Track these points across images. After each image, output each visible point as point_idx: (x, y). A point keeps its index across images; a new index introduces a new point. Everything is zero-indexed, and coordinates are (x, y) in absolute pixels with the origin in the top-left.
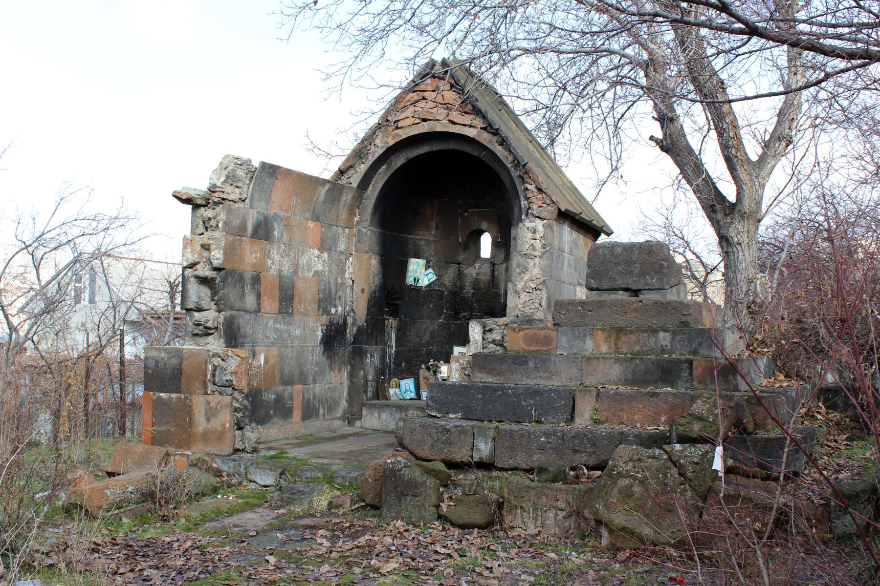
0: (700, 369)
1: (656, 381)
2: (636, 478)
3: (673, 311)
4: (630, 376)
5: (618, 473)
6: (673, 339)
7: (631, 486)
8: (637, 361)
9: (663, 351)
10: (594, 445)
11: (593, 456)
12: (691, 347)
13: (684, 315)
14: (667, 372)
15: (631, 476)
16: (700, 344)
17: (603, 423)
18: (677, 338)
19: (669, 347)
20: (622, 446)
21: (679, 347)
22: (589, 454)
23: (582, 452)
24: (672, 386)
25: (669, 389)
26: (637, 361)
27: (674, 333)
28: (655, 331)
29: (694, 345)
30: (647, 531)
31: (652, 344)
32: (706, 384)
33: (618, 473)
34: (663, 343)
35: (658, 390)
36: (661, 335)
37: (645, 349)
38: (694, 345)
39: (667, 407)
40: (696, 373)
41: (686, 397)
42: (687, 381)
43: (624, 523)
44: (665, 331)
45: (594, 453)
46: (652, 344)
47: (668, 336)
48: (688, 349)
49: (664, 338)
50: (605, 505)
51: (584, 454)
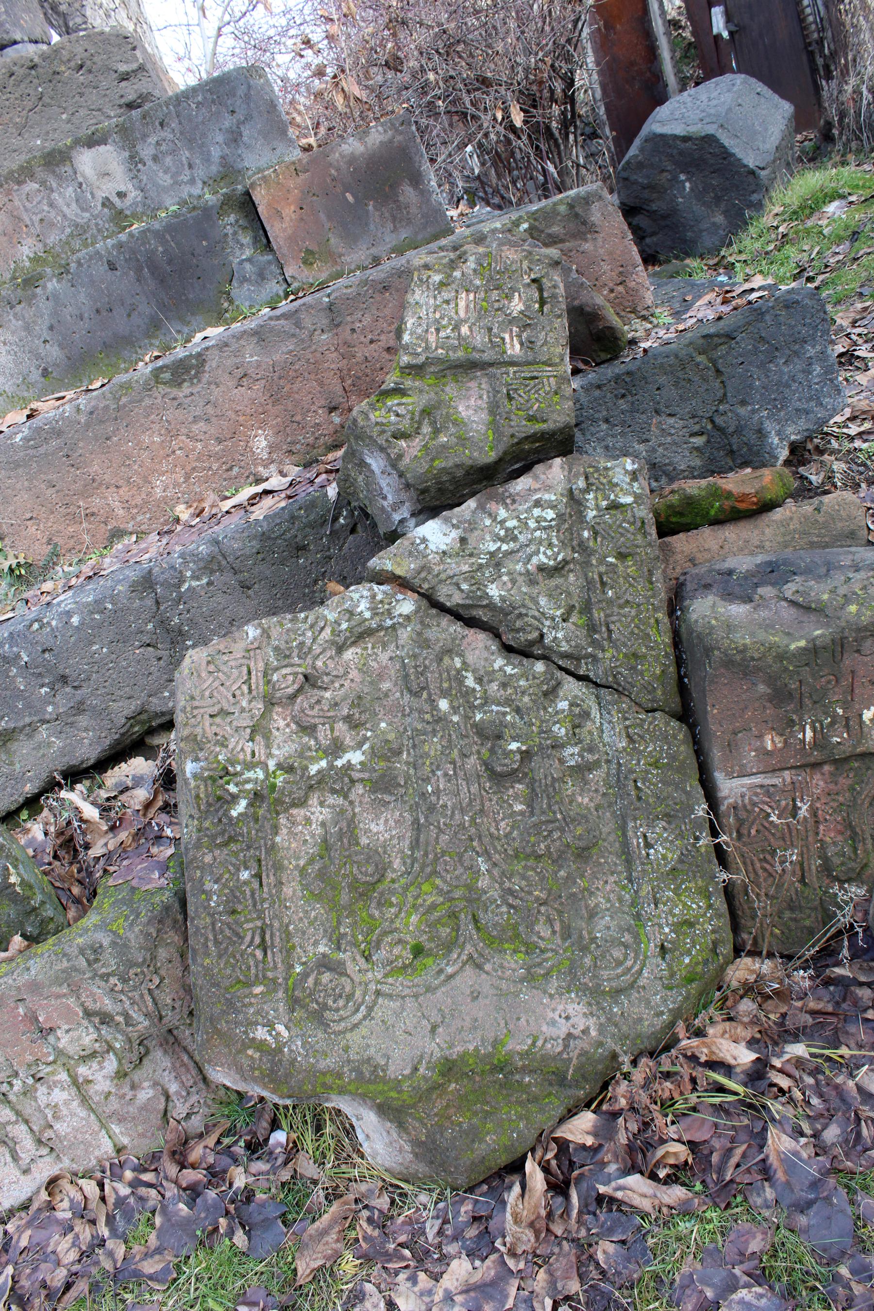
0: (289, 211)
1: (155, 326)
2: (339, 782)
3: (81, 77)
4: (54, 352)
5: (257, 797)
6: (134, 161)
7: (349, 830)
8: (52, 285)
9: (120, 218)
10: (64, 679)
11: (83, 720)
12: (207, 160)
13: (125, 77)
14: (177, 272)
15: (321, 782)
16: (235, 138)
17: (47, 569)
18: (146, 151)
19: (133, 194)
20: (195, 657)
21: (165, 180)
22: (63, 722)
23: (31, 729)
24: (219, 318)
25: (214, 332)
26: (52, 285)
27: (128, 137)
28: (56, 160)
29: (216, 153)
30: (561, 1021)
31: (72, 211)
32: (332, 257)
33: (257, 797)
34: (107, 189)
35: (180, 352)
36: (87, 161)
37: (52, 239)
38: (216, 153)
39: (246, 396)
40: (277, 231)
41: (307, 321)
42: (262, 276)
43: (434, 1048)
44: (92, 142)
45: (79, 708)
46: (72, 211)
47: (109, 156)
48: (200, 172)
49: (102, 170)
50: (294, 1003)
51: (43, 732)
